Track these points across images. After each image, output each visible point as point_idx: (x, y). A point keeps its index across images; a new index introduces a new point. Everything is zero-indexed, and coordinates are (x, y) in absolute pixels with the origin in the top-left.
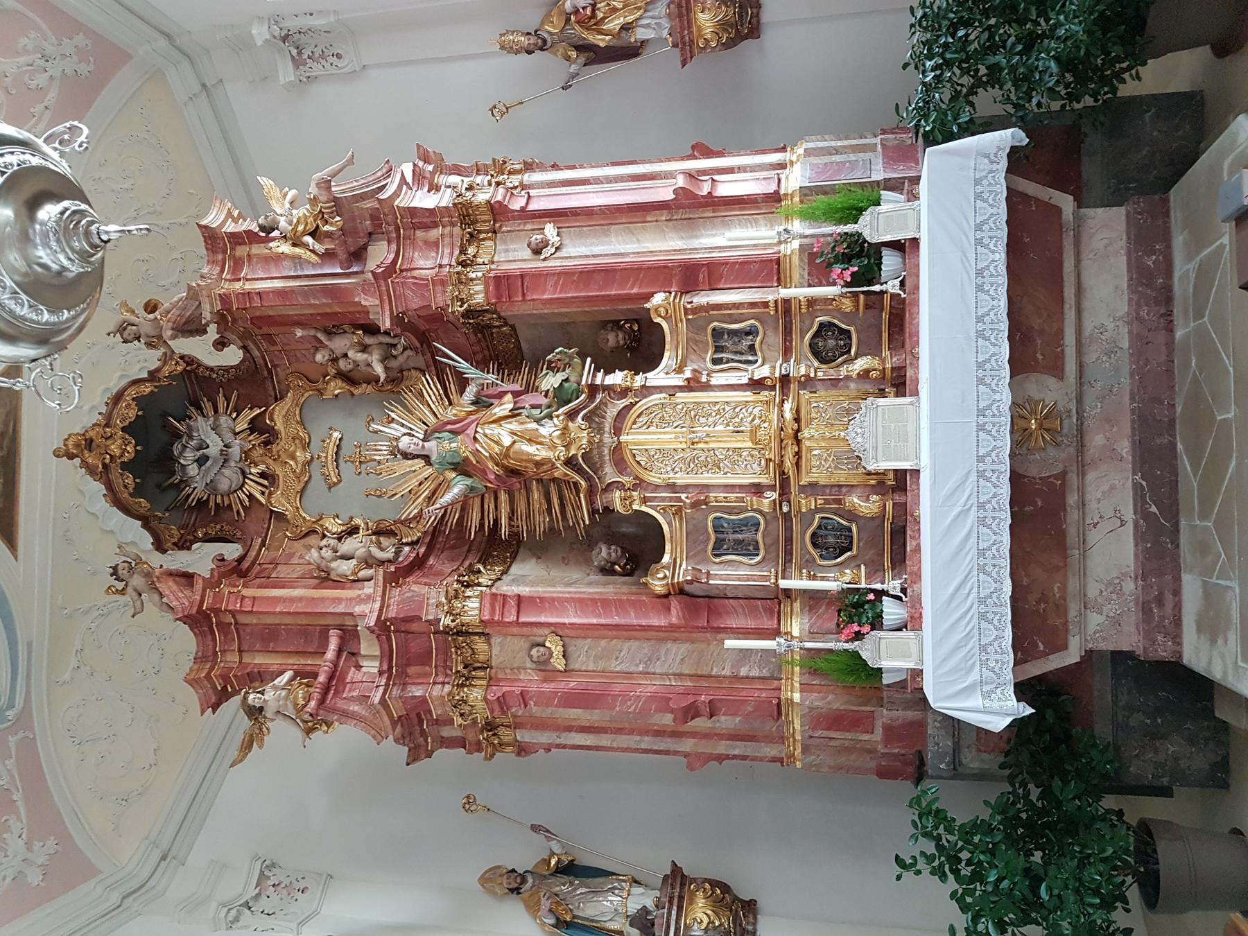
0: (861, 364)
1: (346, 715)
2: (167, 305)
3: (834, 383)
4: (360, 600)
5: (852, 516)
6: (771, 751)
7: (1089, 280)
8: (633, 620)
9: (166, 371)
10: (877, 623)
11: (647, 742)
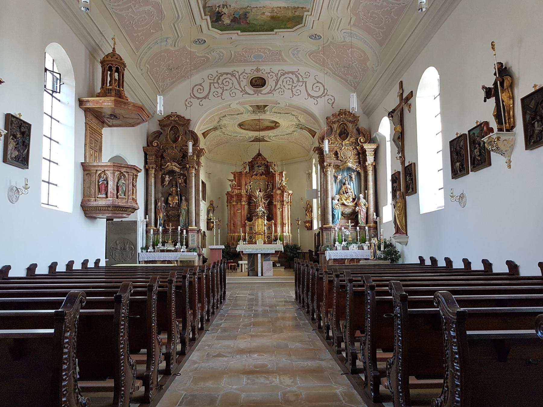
0: (266, 240)
1: (232, 190)
2: (275, 167)
3: (265, 238)
4: (244, 190)
5: (253, 239)
6: (229, 232)
7: (273, 257)
8: (243, 219)
9: (269, 163)
10: (243, 241)
11: (229, 219)
